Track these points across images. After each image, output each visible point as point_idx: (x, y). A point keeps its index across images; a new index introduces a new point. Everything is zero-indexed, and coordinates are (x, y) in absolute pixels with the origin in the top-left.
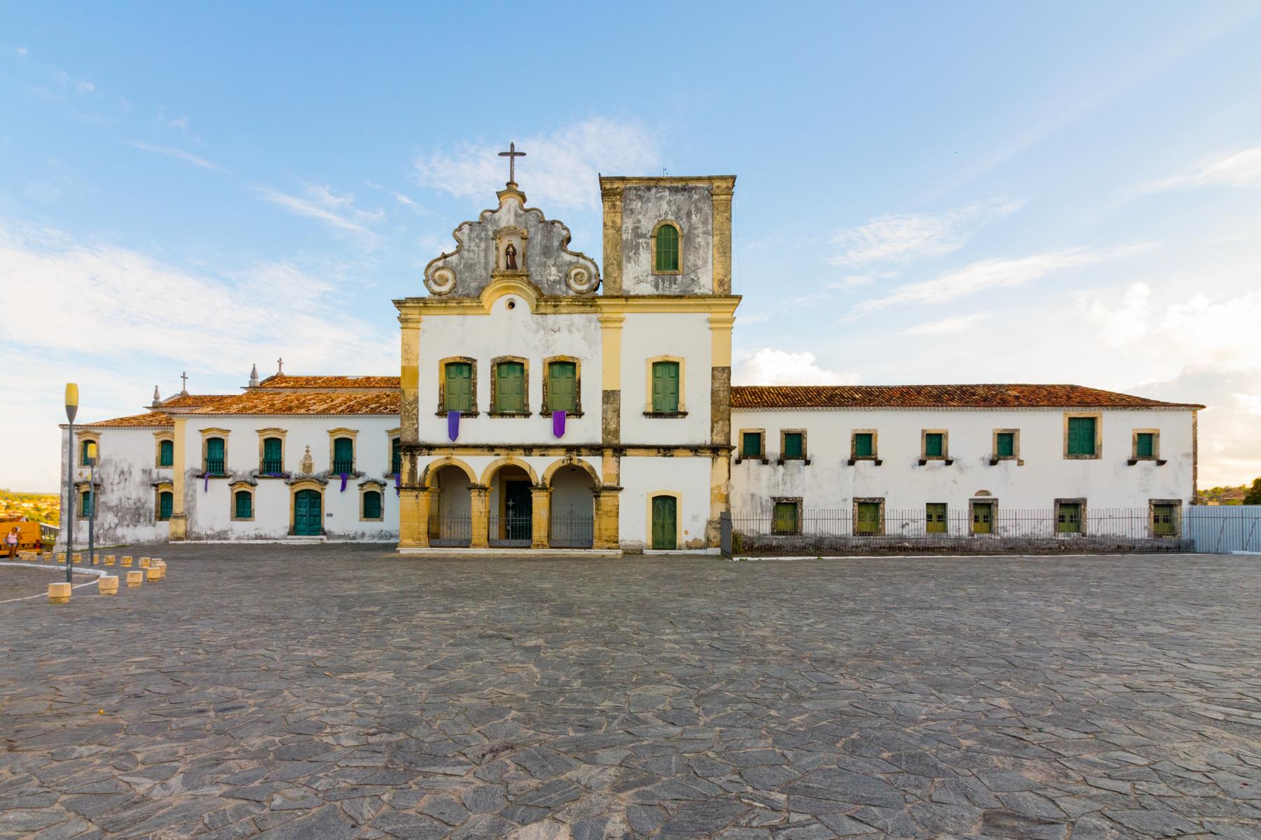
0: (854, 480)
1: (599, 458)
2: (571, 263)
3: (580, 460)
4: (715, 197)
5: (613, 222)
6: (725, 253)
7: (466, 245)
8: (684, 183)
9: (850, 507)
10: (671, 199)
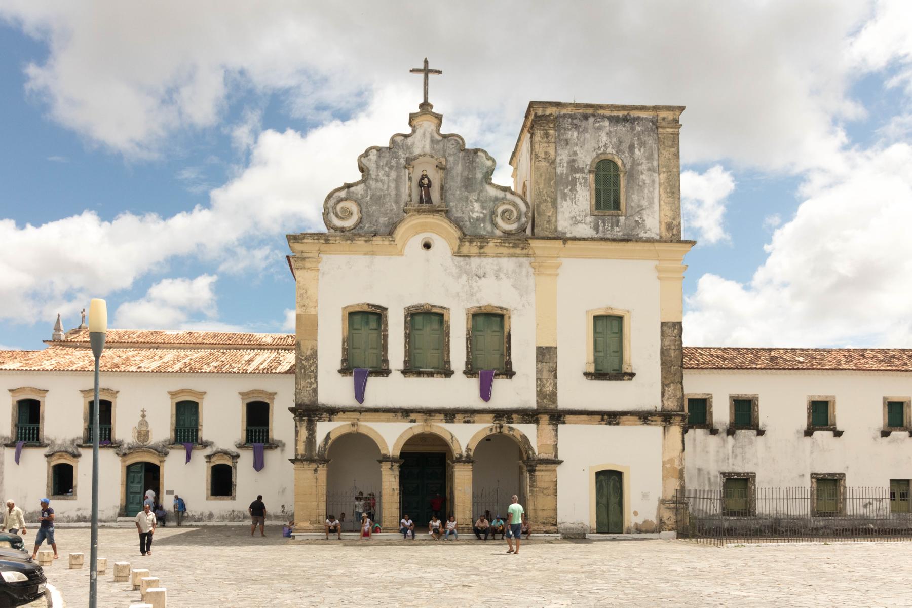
0: (812, 453)
1: (533, 426)
2: (496, 199)
3: (511, 429)
4: (660, 130)
5: (546, 153)
6: (673, 193)
7: (373, 173)
8: (626, 113)
9: (807, 484)
10: (612, 130)
